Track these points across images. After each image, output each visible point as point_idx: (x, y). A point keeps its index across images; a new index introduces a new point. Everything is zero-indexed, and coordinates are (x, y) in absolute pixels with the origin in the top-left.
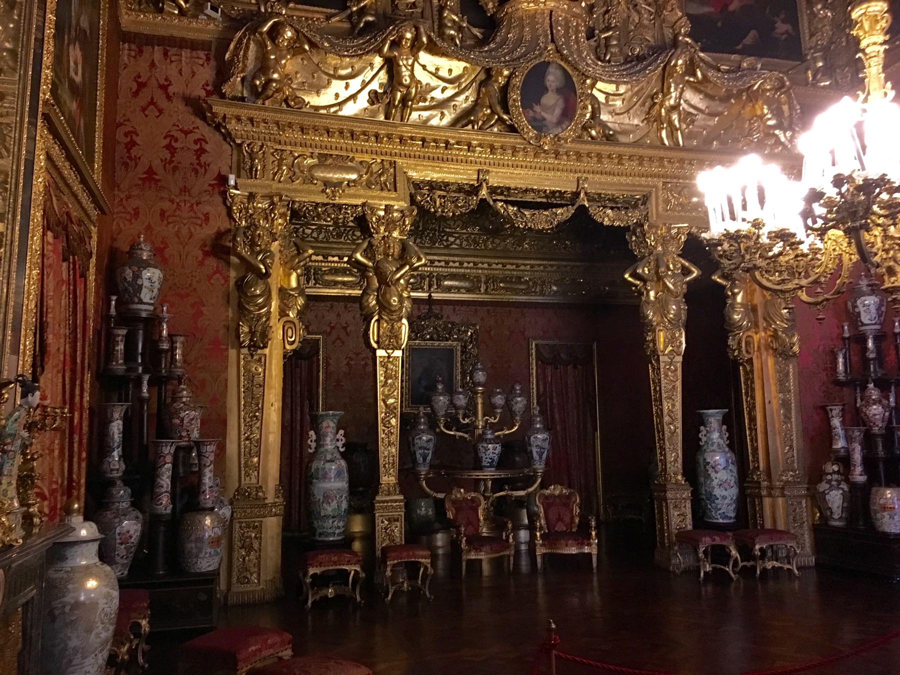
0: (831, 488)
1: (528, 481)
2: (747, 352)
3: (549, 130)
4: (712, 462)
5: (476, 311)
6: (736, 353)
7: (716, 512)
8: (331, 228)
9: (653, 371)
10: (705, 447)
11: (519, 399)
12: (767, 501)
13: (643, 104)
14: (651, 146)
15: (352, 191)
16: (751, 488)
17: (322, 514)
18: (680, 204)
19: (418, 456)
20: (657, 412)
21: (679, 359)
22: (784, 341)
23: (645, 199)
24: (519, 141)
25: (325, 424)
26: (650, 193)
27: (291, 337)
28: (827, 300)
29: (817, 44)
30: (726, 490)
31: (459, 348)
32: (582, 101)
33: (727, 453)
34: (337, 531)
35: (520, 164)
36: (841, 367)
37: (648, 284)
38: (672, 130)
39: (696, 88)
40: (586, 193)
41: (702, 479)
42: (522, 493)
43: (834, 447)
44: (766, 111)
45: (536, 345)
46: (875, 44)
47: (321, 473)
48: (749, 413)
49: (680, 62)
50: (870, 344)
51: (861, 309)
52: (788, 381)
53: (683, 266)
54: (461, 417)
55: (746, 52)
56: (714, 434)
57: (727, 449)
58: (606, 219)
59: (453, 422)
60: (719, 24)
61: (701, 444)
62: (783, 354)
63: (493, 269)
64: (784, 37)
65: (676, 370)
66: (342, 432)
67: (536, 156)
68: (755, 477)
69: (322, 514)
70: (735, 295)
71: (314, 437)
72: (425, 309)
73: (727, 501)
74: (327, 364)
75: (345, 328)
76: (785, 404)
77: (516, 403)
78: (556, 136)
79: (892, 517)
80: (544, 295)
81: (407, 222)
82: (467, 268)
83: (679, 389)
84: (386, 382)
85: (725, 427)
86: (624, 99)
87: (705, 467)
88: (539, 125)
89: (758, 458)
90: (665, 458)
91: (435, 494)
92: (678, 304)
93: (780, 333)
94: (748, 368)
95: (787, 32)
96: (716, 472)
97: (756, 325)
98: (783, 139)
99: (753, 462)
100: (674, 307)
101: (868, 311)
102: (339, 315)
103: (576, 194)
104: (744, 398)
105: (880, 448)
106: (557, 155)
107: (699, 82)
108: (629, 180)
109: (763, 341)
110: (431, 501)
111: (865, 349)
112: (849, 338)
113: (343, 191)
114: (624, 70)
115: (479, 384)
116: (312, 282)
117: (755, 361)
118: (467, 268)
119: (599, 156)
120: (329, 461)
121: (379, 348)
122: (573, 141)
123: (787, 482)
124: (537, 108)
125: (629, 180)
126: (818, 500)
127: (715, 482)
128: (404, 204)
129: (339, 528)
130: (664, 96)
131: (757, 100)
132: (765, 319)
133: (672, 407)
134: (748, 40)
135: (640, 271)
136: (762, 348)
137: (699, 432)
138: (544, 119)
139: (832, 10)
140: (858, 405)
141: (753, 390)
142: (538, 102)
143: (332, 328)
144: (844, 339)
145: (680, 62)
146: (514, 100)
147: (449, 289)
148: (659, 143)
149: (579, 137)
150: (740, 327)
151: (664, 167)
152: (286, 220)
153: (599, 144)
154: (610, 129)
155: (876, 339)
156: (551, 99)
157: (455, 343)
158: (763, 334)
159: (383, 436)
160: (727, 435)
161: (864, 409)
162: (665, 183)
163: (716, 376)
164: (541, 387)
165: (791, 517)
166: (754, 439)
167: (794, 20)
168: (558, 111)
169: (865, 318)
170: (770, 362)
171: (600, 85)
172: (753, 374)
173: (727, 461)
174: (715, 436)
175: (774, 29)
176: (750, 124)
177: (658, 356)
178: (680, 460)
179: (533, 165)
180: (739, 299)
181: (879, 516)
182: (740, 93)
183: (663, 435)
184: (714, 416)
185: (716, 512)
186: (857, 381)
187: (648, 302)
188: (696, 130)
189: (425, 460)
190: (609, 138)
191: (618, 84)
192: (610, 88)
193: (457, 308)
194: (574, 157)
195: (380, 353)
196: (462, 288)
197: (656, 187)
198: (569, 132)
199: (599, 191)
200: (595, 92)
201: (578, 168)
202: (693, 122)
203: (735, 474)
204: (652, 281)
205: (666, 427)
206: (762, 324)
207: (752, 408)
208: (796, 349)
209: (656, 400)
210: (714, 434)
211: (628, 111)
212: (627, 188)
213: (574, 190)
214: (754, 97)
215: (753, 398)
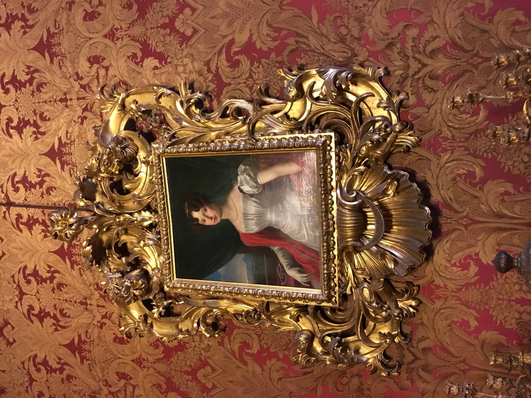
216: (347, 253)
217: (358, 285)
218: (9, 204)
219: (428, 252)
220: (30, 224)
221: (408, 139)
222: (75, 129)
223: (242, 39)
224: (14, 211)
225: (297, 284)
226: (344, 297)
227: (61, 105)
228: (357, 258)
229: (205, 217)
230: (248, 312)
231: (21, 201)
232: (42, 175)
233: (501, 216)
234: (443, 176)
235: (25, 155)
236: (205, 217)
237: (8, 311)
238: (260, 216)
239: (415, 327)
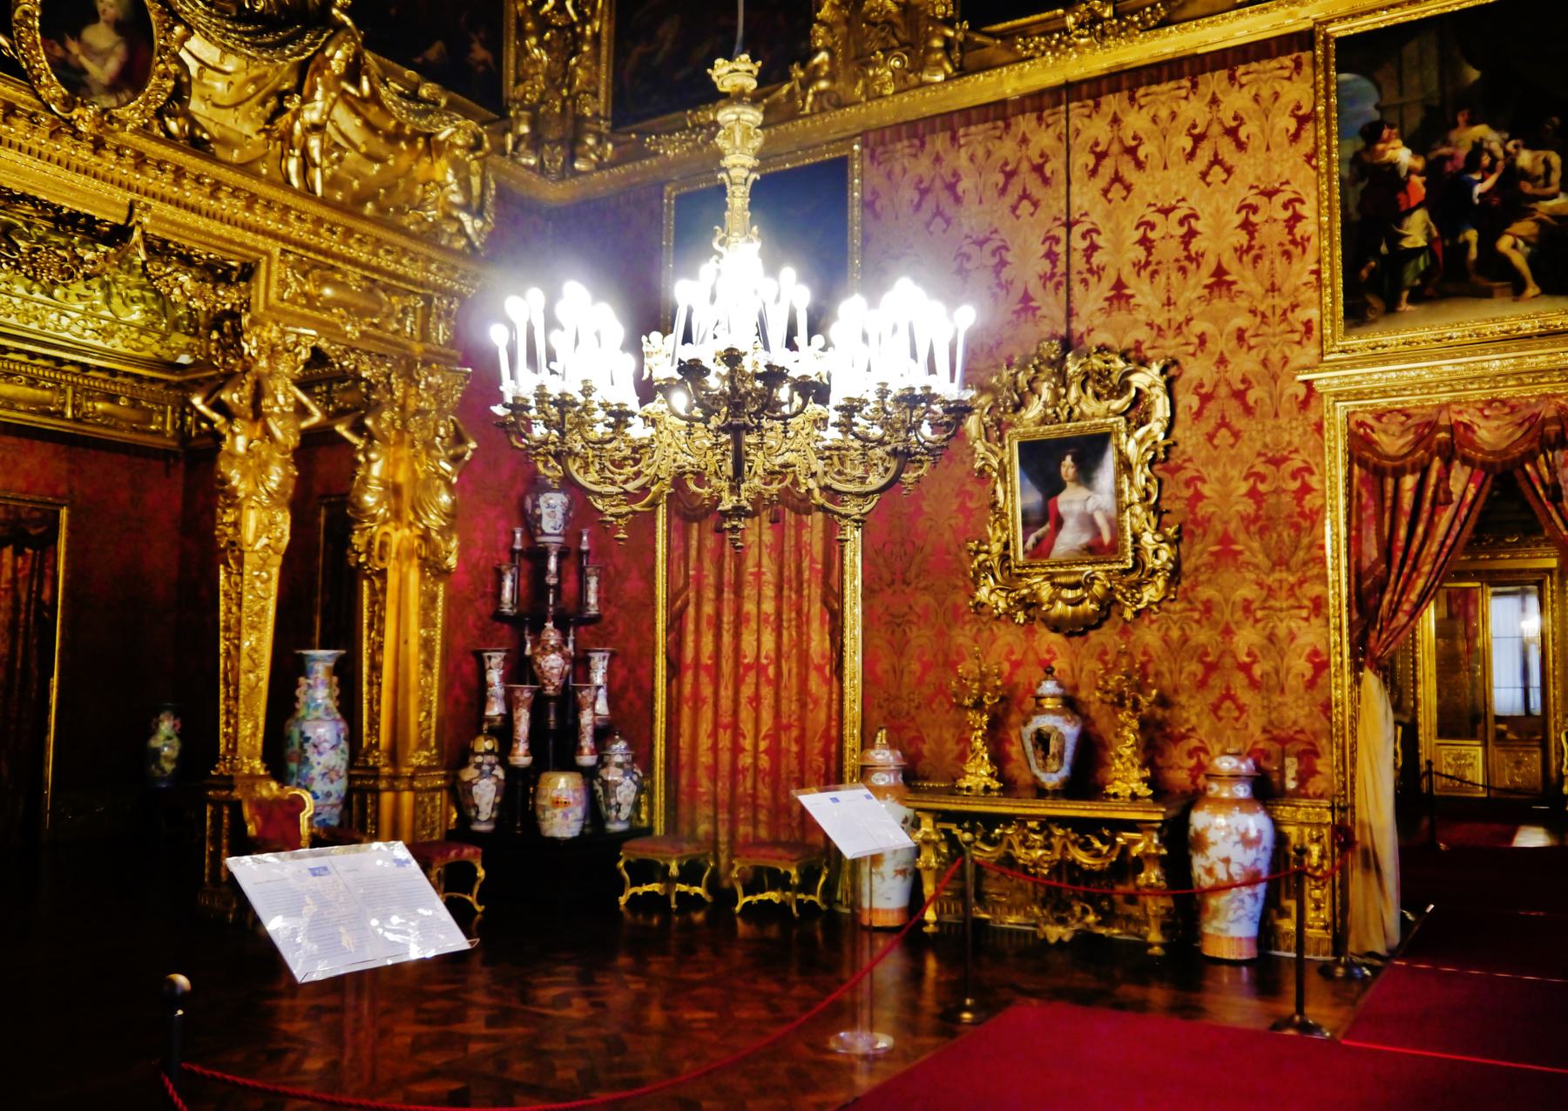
0: (482, 775)
3: (91, 94)
6: (362, 559)
9: (228, 578)
12: (387, 798)
13: (263, 103)
14: (271, 182)
18: (305, 295)
20: (228, 652)
21: (278, 560)
22: (437, 546)
23: (248, 272)
24: (24, 96)
26: (257, 262)
28: (634, 512)
29: (524, 97)
30: (332, 782)
32: (162, 61)
35: (17, 141)
36: (507, 594)
37: (238, 421)
38: (306, 164)
39: (355, 106)
40: (143, 233)
41: (293, 766)
43: (489, 713)
44: (450, 178)
46: (743, 166)
48: (372, 657)
49: (339, 55)
50: (552, 564)
51: (544, 510)
52: (435, 609)
53: (298, 401)
55: (428, 73)
56: (318, 692)
57: (338, 716)
58: (177, 291)
60: (393, 11)
62: (432, 567)
64: (481, 68)
65: (269, 579)
67: (53, 135)
70: (369, 461)
76: (427, 644)
78: (105, 111)
79: (565, 815)
83: (271, 613)
85: (335, 679)
86: (231, 83)
87: (301, 746)
88: (75, 82)
89: (378, 731)
90: (236, 731)
92: (285, 464)
93: (433, 534)
94: (378, 585)
95: (484, 62)
96: (320, 754)
97: (397, 515)
98: (469, 230)
101: (552, 515)
104: (365, 632)
105: (552, 717)
106: (98, 145)
107: (363, 100)
108: (225, 230)
109: (405, 544)
111: (544, 570)
112: (520, 551)
114: (247, 34)
119: (179, 173)
122: (135, 131)
123: (419, 768)
124: (74, 47)
125: (225, 230)
126: (460, 795)
127: (316, 772)
130: (304, 101)
131: (439, 157)
132: (414, 509)
133: (253, 644)
134: (434, 52)
135: (225, 396)
137: (297, 686)
138: (84, 71)
139: (549, 52)
140: (528, 651)
141: (382, 620)
142: (77, 36)
144: (513, 552)
145: (339, 55)
146: (26, 13)
148: (280, 179)
149: (146, 126)
150: (373, 518)
151: (286, 223)
153: (179, 148)
154: (204, 130)
155: (561, 556)
156: (100, 36)
161: (539, 659)
162: (284, 252)
163: (326, 590)
165: (419, 822)
166: (375, 701)
167: (495, 46)
168: (112, 65)
169: (548, 525)
170: (414, 576)
171: (196, 43)
175: (471, 50)
176: (425, 191)
177: (242, 552)
178: (260, 735)
179: (46, 152)
180: (376, 470)
181: (548, 814)
182: (415, 134)
183: (237, 690)
184: (321, 660)
186: (530, 618)
187: (232, 455)
188: (343, 174)
190: (197, 144)
191: (226, 50)
192: (211, 54)
194: (132, 161)
197: (268, 253)
198: (132, 113)
199: (168, 237)
200: (183, 54)
201: (135, 184)
202: (340, 159)
204: (244, 418)
205: (243, 678)
207: (378, 648)
208: (452, 561)
209: (227, 629)
210: (318, 692)
211: (235, 106)
212: (219, 243)
213: (121, 222)
214: (433, 147)
215: (381, 633)
216: (1050, 577)
217: (1029, 586)
218: (1069, 225)
219: (1056, 630)
220: (1051, 256)
221: (1128, 615)
222: (1141, 316)
223: (1206, 490)
224: (1061, 233)
225: (1025, 542)
226: (1019, 575)
227: (1164, 298)
228: (1047, 584)
229: (1068, 467)
230: (996, 503)
231: (1073, 244)
232: (1097, 272)
233: (1081, 670)
234: (1106, 636)
235: (1118, 247)
236: (1068, 467)
237: (960, 225)
238: (1071, 513)
239: (1005, 622)
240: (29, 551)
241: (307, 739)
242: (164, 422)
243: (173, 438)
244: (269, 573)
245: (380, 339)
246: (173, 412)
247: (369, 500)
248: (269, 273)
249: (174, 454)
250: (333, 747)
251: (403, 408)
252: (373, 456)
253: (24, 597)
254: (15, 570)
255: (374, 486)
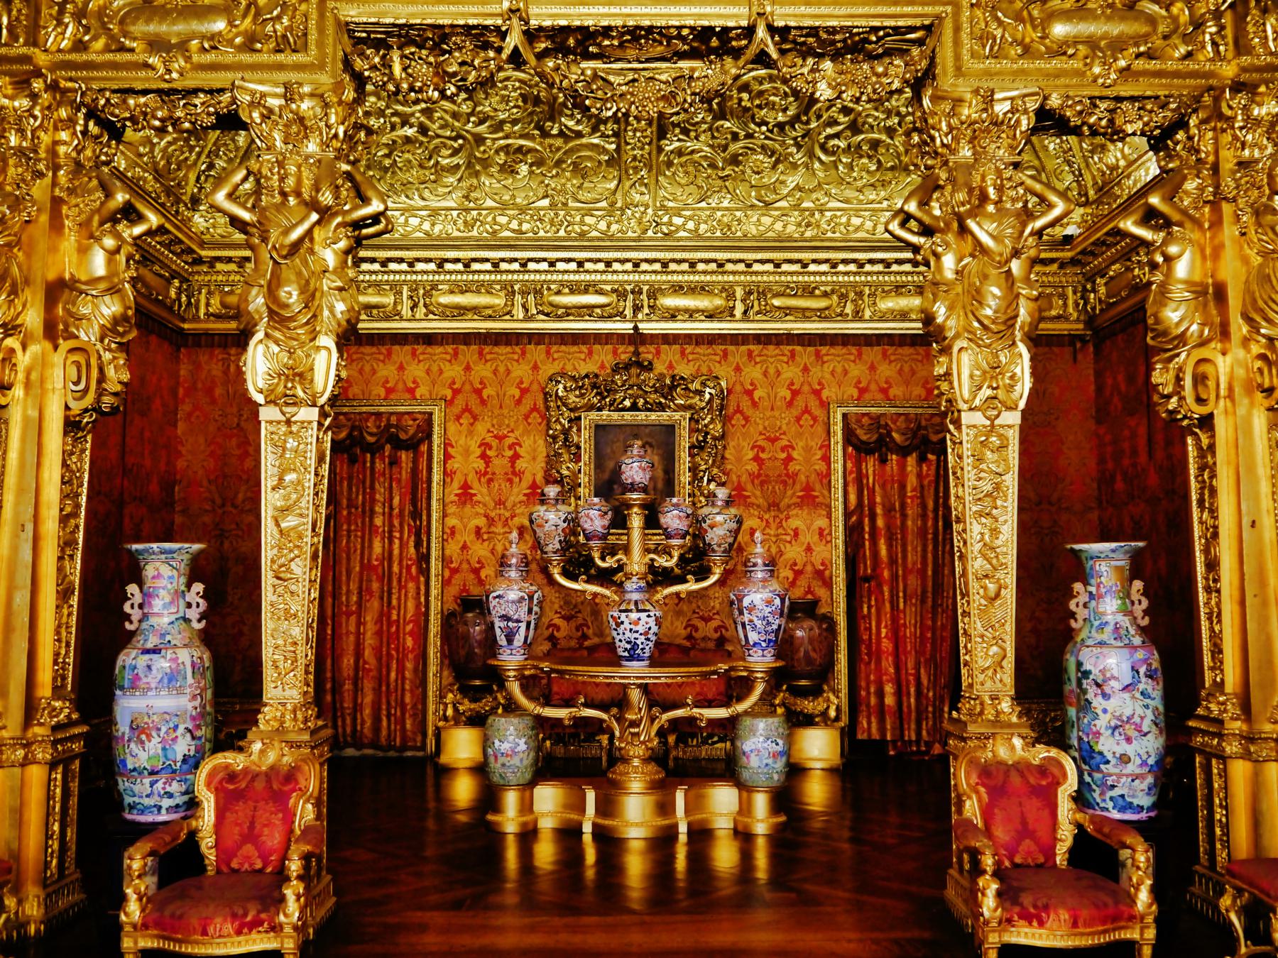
1: (735, 688)
2: (1200, 401)
4: (1095, 671)
5: (726, 354)
6: (1174, 401)
7: (1102, 794)
8: (455, 213)
10: (1083, 635)
11: (719, 518)
12: (1240, 770)
15: (210, 58)
16: (1205, 733)
17: (130, 766)
19: (498, 632)
21: (1013, 418)
25: (149, 571)
27: (76, 383)
30: (1129, 740)
31: (686, 424)
33: (1135, 648)
34: (166, 803)
41: (1072, 712)
42: (721, 713)
45: (845, 416)
47: (128, 675)
48: (1206, 551)
54: (596, 555)
56: (1107, 604)
57: (1137, 641)
59: (578, 564)
61: (1073, 624)
63: (756, 273)
65: (1004, 447)
66: (199, 587)
68: (1213, 707)
69: (130, 766)
70: (1168, 259)
71: (138, 599)
72: (625, 352)
73: (1131, 768)
74: (447, 456)
75: (478, 392)
77: (712, 527)
80: (861, 320)
81: (333, 119)
82: (705, 272)
84: (281, 479)
85: (1138, 585)
87: (1079, 684)
91: (539, 710)
96: (1106, 696)
97: (1225, 333)
99: (1212, 669)
100: (996, 291)
102: (468, 368)
103: (750, 31)
109: (1241, 372)
110: (528, 721)
113: (188, 59)
115: (633, 487)
116: (421, 311)
117: (1220, 424)
118: (705, 272)
120: (147, 651)
121: (267, 403)
127: (1102, 723)
128: (325, 79)
129: (170, 796)
136: (1237, 390)
137: (1071, 595)
143: (456, 392)
147: (673, 315)
152: (74, 133)
157: (677, 416)
158: (1241, 353)
159: (274, 598)
160: (1145, 603)
164: (853, 498)
172: (1214, 455)
173: (1135, 670)
174: (1110, 606)
180: (1181, 269)
184: (1106, 559)
185: (1102, 794)
189: (510, 639)
193: (689, 349)
195: (268, 414)
196: (698, 311)
203: (1157, 703)
206: (1239, 328)
207: (1213, 535)
210: (1107, 604)
213: (744, 23)
215: (1213, 512)
240: (930, 456)
241: (1086, 674)
242: (1065, 305)
243: (1078, 320)
244: (1000, 436)
245: (1159, 74)
246: (1075, 293)
247: (1172, 315)
248: (957, 29)
249: (1081, 338)
250: (1126, 688)
251: (1215, 168)
252: (1173, 250)
253: (931, 505)
254: (920, 476)
255: (1179, 292)
